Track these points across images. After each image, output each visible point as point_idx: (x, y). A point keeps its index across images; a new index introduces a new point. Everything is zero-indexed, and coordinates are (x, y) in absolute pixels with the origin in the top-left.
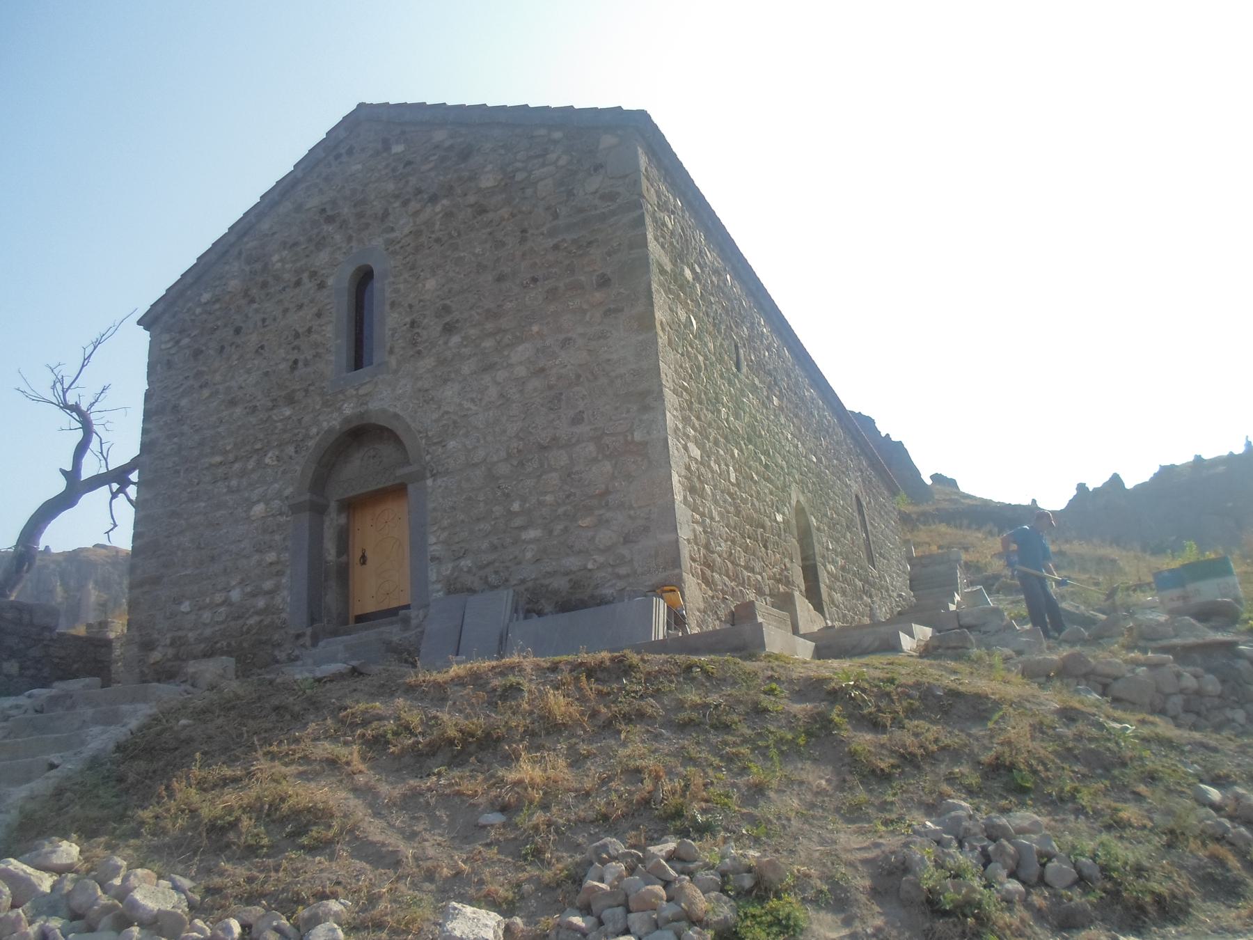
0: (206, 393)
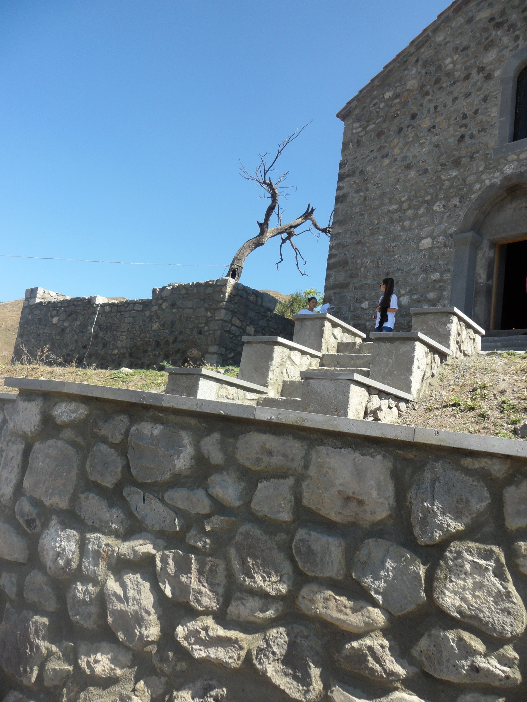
0: (386, 161)
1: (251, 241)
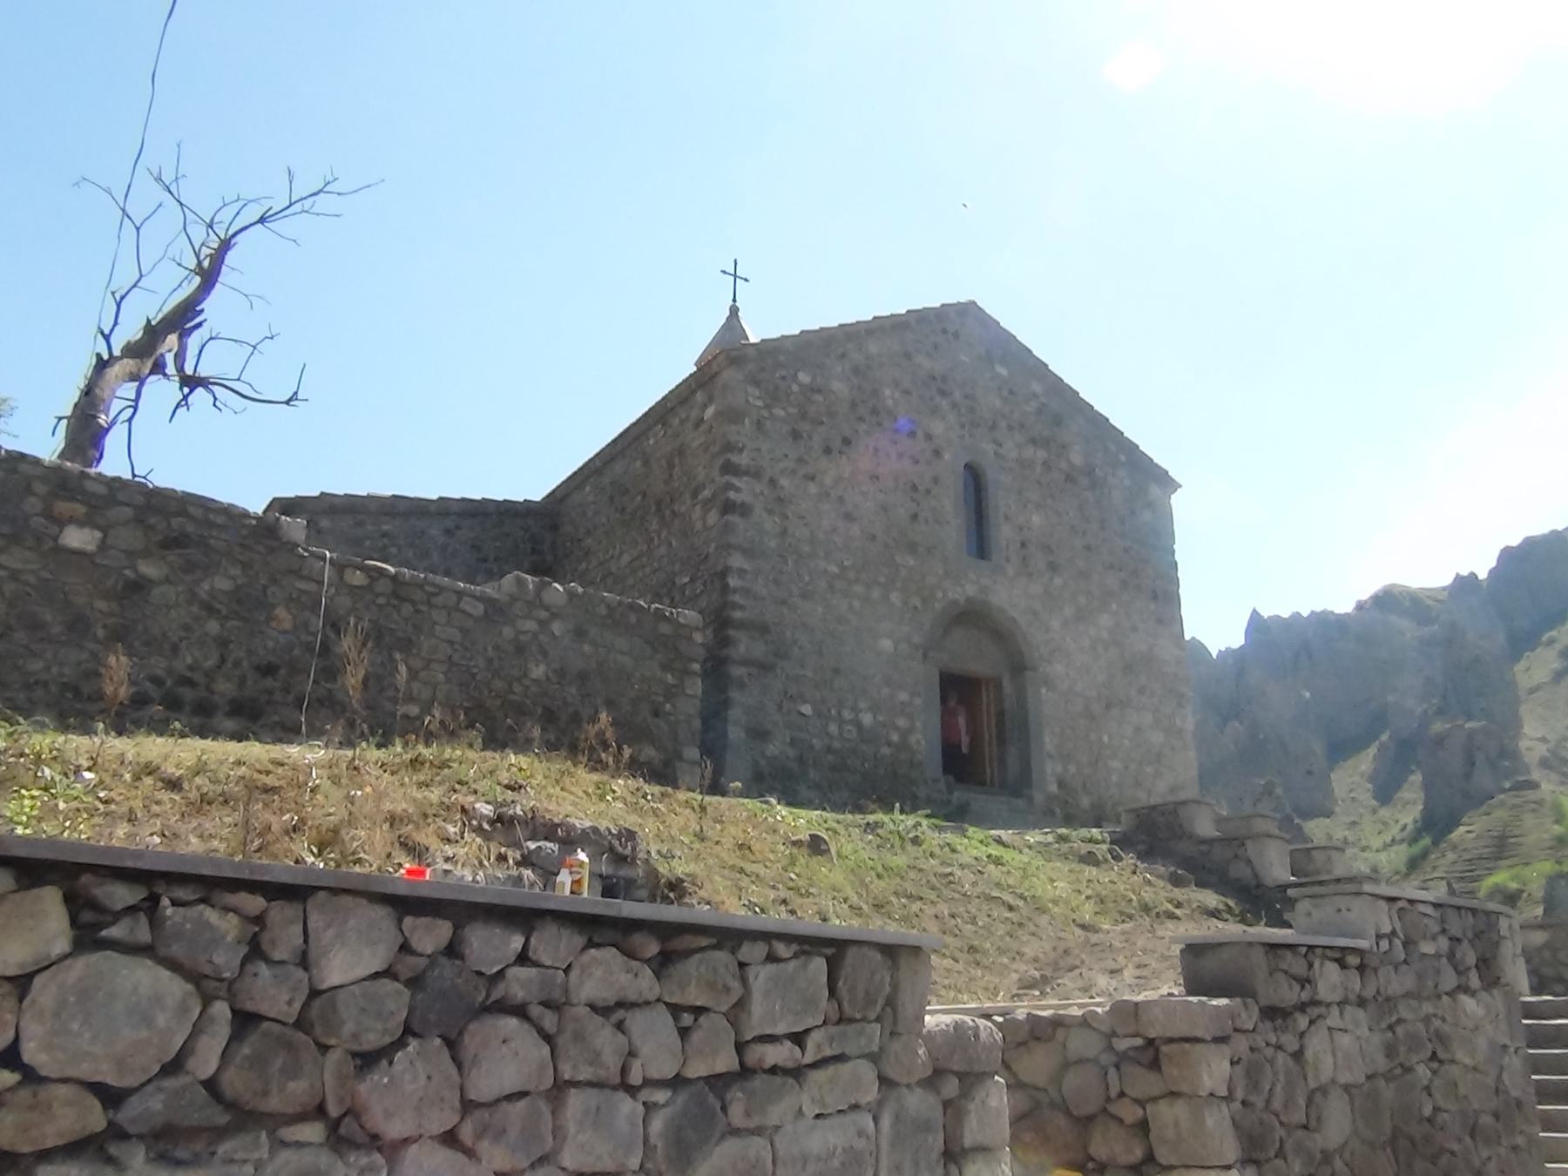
0: (813, 488)
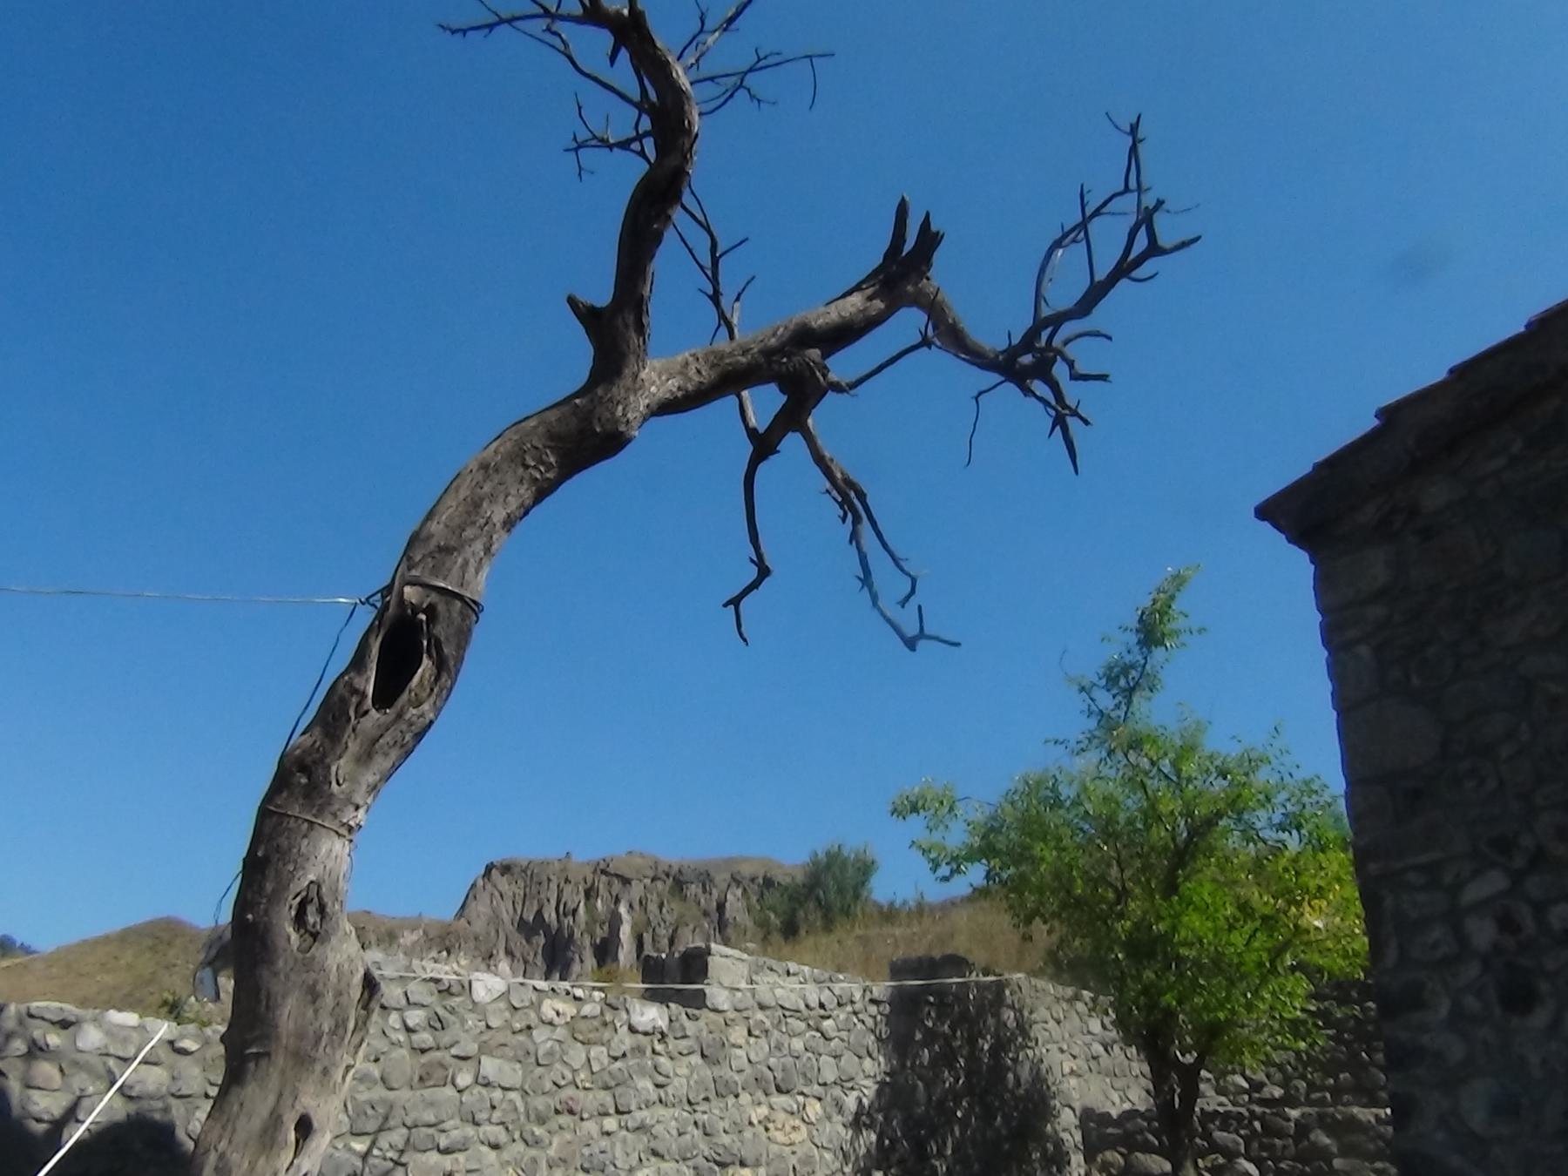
1: (532, 423)
